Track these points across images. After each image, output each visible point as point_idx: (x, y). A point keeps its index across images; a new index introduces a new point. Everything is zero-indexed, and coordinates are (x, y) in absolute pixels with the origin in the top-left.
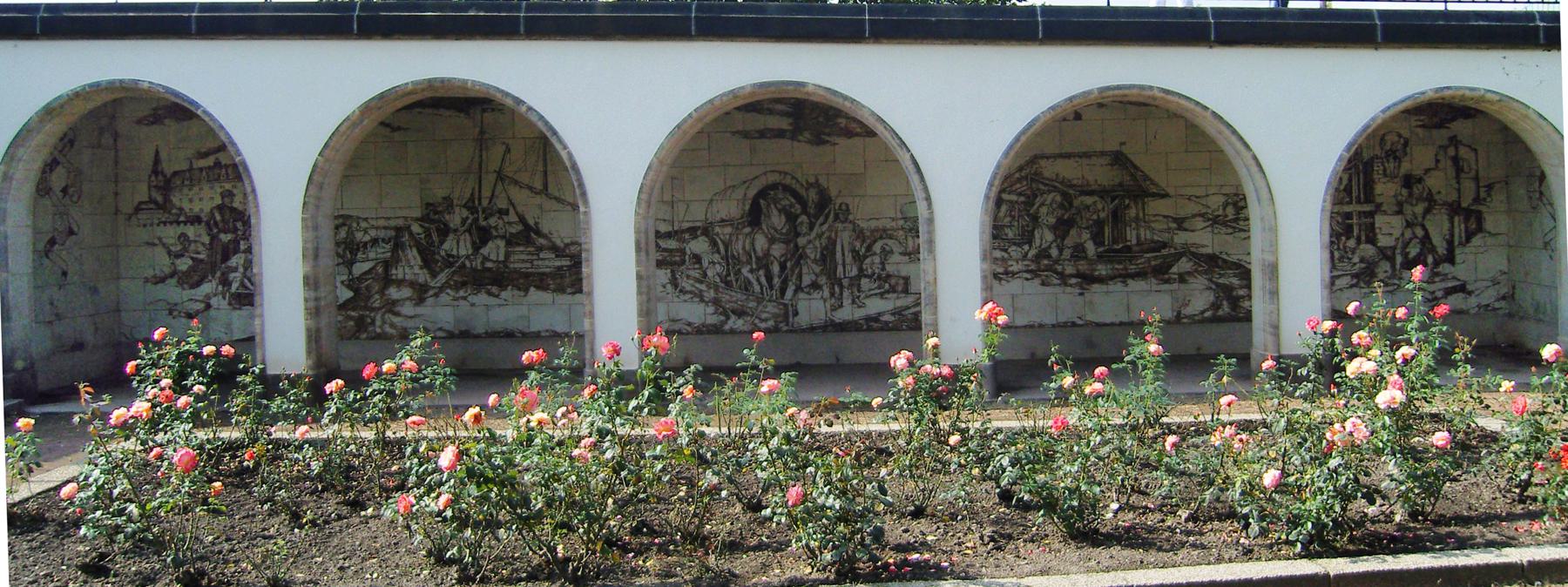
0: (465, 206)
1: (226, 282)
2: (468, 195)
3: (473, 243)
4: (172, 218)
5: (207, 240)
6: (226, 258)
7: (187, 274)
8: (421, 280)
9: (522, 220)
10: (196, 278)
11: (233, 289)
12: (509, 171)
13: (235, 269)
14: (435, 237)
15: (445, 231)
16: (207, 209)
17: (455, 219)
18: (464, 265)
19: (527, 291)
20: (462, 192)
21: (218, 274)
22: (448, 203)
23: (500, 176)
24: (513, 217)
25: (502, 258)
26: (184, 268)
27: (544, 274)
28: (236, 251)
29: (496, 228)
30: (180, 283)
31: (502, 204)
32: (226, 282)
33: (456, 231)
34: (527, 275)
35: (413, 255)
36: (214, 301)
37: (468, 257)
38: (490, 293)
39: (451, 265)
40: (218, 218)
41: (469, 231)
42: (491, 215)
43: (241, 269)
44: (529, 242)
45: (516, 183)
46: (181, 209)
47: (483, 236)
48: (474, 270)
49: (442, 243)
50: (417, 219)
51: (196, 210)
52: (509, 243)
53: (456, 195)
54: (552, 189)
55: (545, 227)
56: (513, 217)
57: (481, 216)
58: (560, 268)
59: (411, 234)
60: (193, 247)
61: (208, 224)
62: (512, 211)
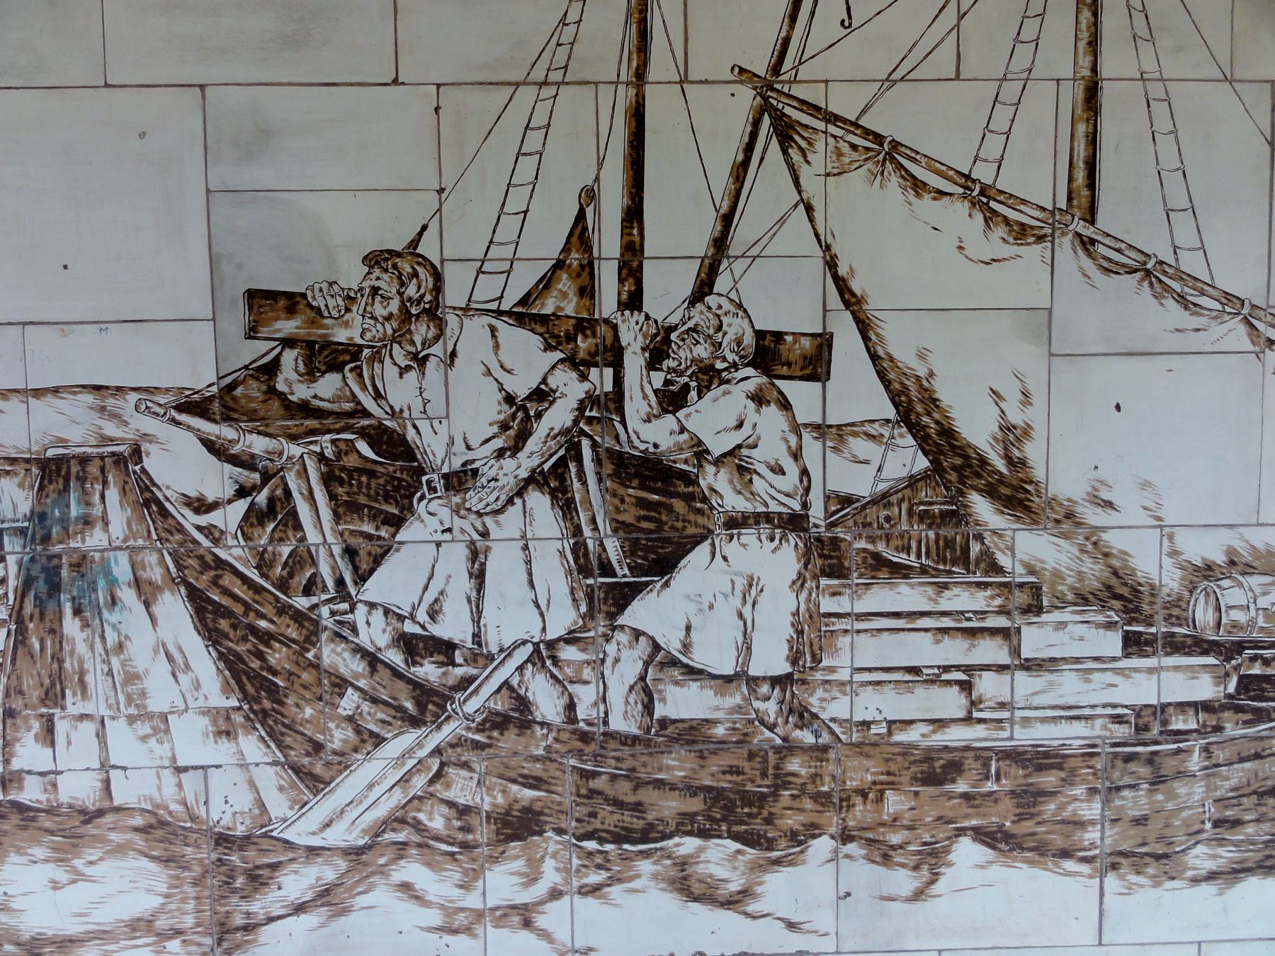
0: (523, 316)
2: (547, 238)
3: (584, 562)
8: (227, 805)
9: (915, 409)
12: (836, 73)
14: (319, 526)
15: (383, 481)
17: (454, 404)
18: (516, 715)
19: (932, 859)
20: (500, 232)
22: (413, 293)
23: (779, 120)
24: (854, 392)
25: (771, 658)
27: (1043, 759)
29: (737, 462)
31: (780, 296)
33: (460, 480)
34: (937, 769)
35: (161, 642)
37: (544, 654)
38: (688, 886)
39: (429, 705)
41: (553, 480)
42: (708, 376)
44: (955, 554)
45: (887, 153)
47: (658, 515)
48: (586, 738)
49: (364, 562)
50: (195, 406)
52: (826, 560)
53: (457, 243)
54: (1125, 213)
55: (1061, 472)
56: (854, 392)
57: (640, 384)
58: (1147, 719)
59: (148, 500)
62: (847, 346)
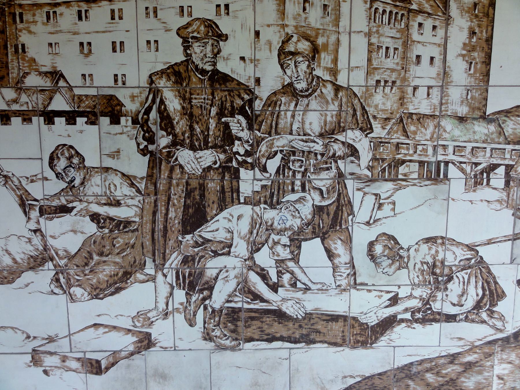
1: (195, 282)
4: (26, 102)
5: (139, 166)
6: (195, 217)
7: (87, 257)
10: (106, 271)
11: (218, 300)
13: (226, 248)
16: (137, 78)
21: (174, 260)
26: (72, 243)
28: (228, 197)
30: (62, 283)
32: (195, 282)
36: (161, 330)
40: (173, 104)
43: (241, 248)
46: (56, 75)
51: (103, 81)
60: (95, 186)
61: (140, 121)
